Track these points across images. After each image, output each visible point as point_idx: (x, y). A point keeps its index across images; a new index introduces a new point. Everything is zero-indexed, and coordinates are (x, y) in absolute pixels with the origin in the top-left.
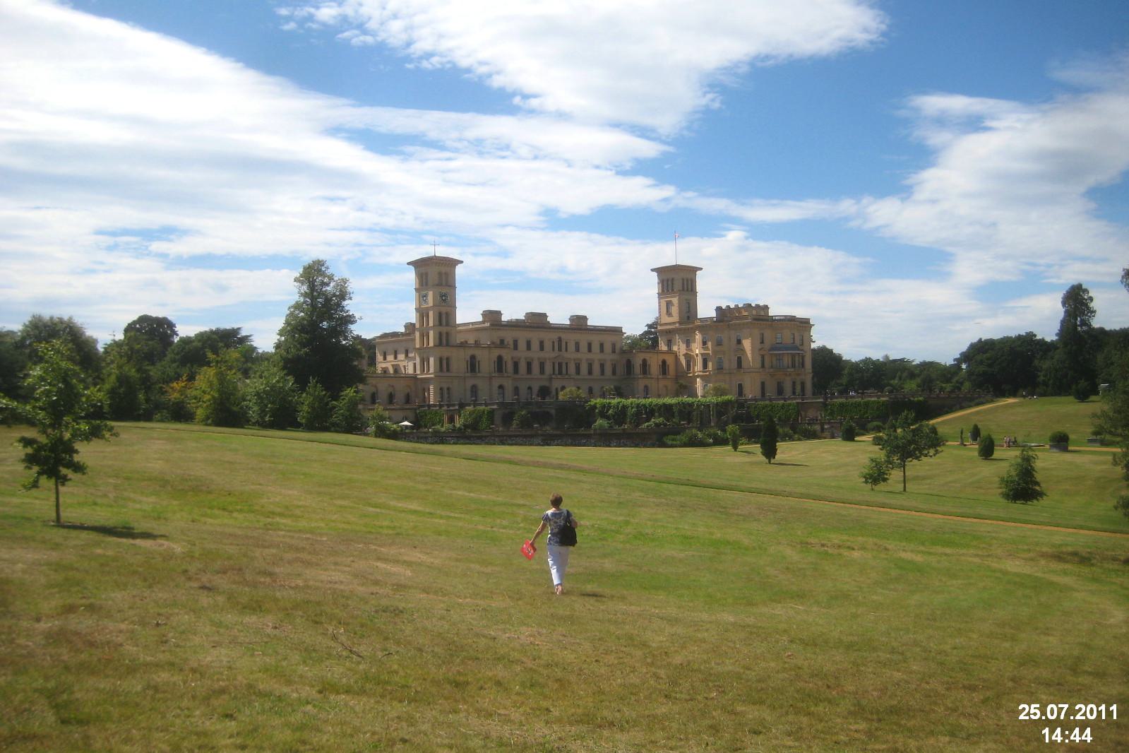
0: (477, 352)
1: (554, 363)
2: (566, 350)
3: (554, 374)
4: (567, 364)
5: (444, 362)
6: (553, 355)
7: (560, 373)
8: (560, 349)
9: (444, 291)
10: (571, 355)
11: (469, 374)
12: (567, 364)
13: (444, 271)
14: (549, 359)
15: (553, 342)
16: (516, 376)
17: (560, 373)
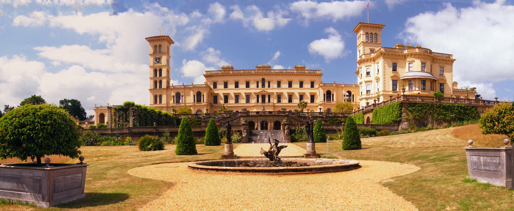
6: (258, 91)
8: (263, 86)
13: (158, 45)
15: (258, 83)
16: (215, 105)
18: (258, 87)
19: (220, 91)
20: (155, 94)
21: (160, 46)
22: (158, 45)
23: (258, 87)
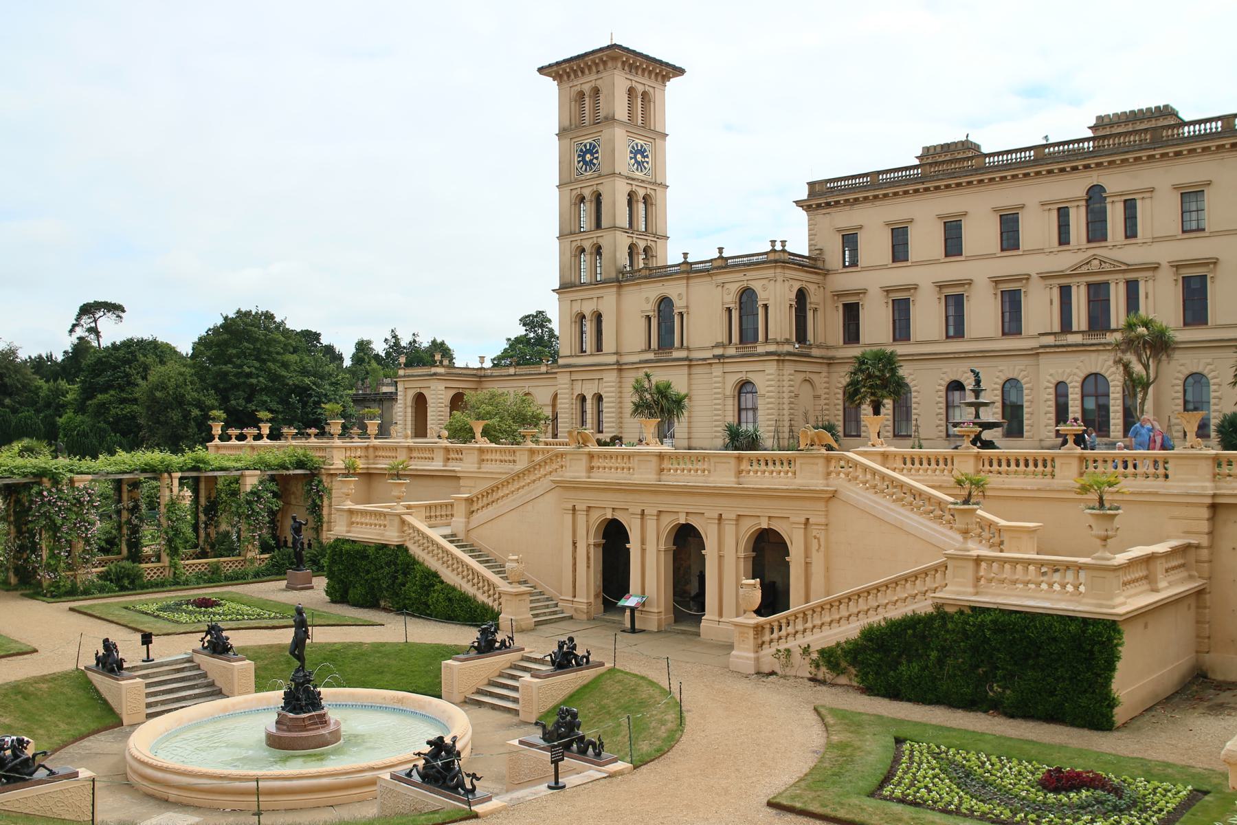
0: (673, 290)
1: (1065, 292)
2: (1131, 231)
3: (1066, 327)
5: (589, 327)
6: (1064, 261)
7: (1099, 321)
8: (1097, 232)
11: (651, 356)
13: (586, 88)
14: (1044, 277)
15: (1063, 214)
17: (1099, 321)
18: (1064, 239)
19: (874, 277)
20: (577, 308)
21: (596, 91)
22: (586, 88)
23: (1064, 239)
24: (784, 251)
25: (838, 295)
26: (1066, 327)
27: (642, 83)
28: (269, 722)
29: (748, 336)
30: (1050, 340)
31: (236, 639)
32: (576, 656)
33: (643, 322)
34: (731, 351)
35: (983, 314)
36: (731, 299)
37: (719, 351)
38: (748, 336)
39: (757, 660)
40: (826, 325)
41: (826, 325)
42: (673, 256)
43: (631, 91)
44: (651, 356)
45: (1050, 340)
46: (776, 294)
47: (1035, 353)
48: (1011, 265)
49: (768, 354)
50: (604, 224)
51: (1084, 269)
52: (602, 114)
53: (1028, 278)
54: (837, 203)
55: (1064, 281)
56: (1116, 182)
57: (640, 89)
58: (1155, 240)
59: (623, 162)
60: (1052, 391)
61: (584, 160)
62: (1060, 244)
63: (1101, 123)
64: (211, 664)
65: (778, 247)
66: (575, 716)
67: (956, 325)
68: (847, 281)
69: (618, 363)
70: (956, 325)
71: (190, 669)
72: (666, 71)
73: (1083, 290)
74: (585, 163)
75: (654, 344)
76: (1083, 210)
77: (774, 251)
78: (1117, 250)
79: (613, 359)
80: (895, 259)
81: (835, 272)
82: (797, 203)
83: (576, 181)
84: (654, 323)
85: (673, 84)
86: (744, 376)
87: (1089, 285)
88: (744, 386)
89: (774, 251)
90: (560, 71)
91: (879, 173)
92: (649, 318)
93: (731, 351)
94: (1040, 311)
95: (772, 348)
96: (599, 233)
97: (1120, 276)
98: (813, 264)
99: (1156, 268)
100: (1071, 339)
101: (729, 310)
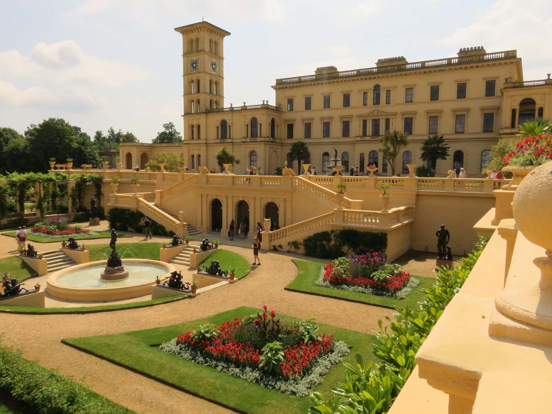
0: (227, 117)
1: (365, 122)
2: (388, 102)
3: (364, 134)
4: (388, 121)
5: (195, 130)
6: (365, 111)
7: (376, 133)
8: (377, 101)
9: (194, 59)
10: (397, 106)
11: (218, 141)
12: (388, 121)
15: (365, 94)
17: (376, 133)
18: (365, 104)
21: (198, 40)
24: (267, 104)
25: (286, 121)
26: (364, 134)
27: (214, 37)
28: (102, 270)
29: (254, 135)
30: (359, 139)
31: (80, 243)
32: (209, 245)
33: (215, 129)
34: (248, 140)
35: (336, 129)
36: (248, 121)
37: (243, 140)
38: (254, 135)
39: (270, 245)
40: (282, 132)
41: (282, 132)
42: (226, 105)
43: (211, 41)
44: (218, 141)
45: (359, 139)
46: (264, 120)
47: (354, 143)
48: (347, 112)
49: (261, 141)
50: (201, 91)
51: (372, 114)
52: (200, 49)
53: (352, 117)
54: (286, 87)
55: (365, 118)
56: (384, 83)
57: (214, 39)
58: (396, 104)
59: (209, 68)
60: (359, 156)
61: (193, 66)
62: (364, 105)
63: (380, 62)
64: (70, 252)
65: (265, 103)
66: (218, 263)
67: (327, 133)
68: (290, 116)
69: (206, 143)
70: (327, 133)
71: (62, 254)
72: (223, 33)
73: (371, 121)
74: (194, 68)
75: (220, 137)
76: (372, 93)
77: (264, 104)
78: (383, 107)
79: (205, 142)
80: (306, 109)
81: (285, 112)
82: (272, 87)
83: (190, 74)
84: (220, 129)
85: (226, 39)
86: (252, 149)
87: (373, 120)
88: (252, 153)
89: (264, 104)
90: (184, 30)
91: (301, 77)
92: (218, 127)
93: (248, 140)
94: (356, 129)
95: (262, 139)
96: (199, 95)
97: (383, 117)
98: (278, 109)
99: (395, 114)
100: (366, 138)
101: (247, 125)
